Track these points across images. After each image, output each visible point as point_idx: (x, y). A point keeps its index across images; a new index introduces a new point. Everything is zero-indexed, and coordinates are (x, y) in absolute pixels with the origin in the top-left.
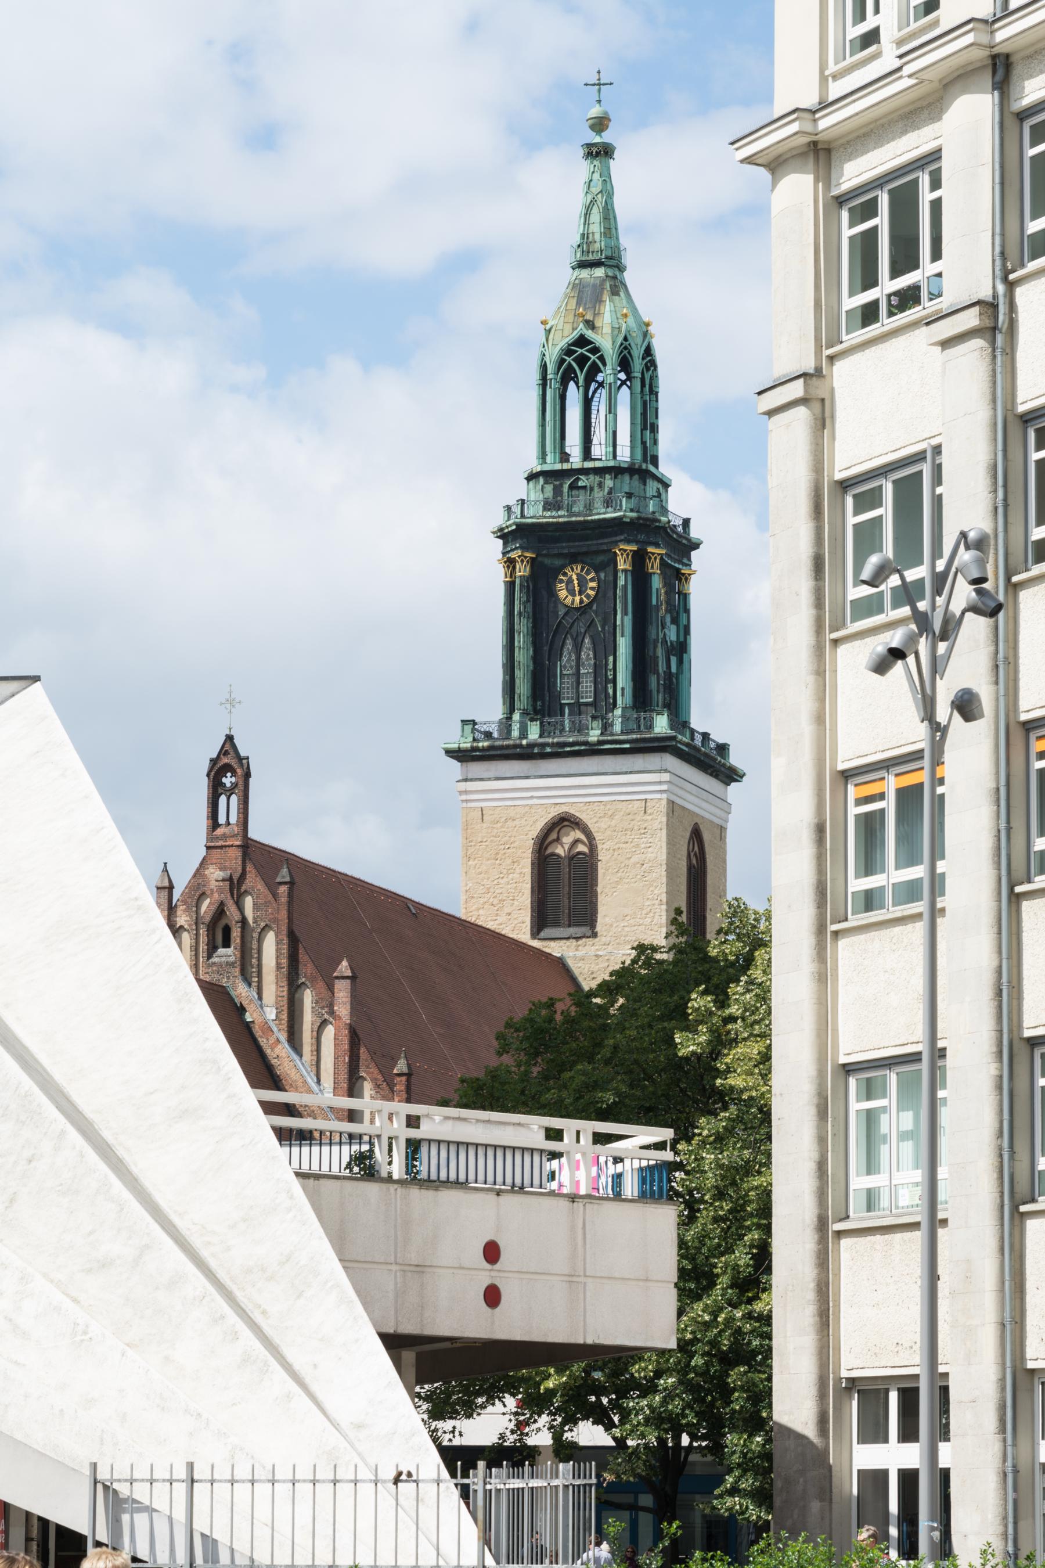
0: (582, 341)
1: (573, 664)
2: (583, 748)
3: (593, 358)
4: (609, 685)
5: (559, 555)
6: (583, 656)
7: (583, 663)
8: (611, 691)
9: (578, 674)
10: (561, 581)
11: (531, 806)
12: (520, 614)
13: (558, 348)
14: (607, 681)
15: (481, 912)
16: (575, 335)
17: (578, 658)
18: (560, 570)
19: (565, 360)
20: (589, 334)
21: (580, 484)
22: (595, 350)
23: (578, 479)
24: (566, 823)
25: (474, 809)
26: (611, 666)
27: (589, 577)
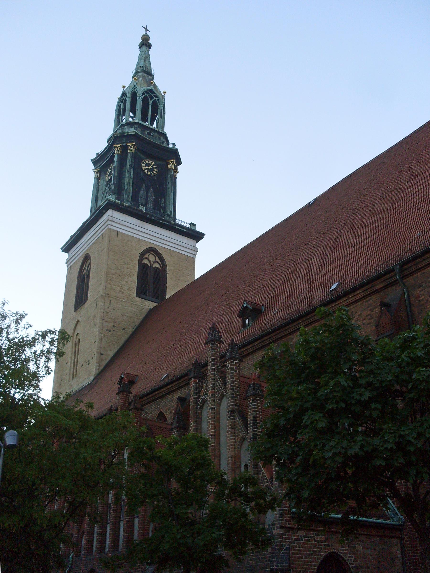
0: (151, 91)
1: (145, 195)
2: (167, 224)
3: (155, 98)
4: (162, 209)
5: (144, 153)
6: (149, 194)
7: (149, 197)
8: (162, 211)
9: (146, 200)
10: (144, 163)
11: (139, 240)
12: (131, 165)
13: (143, 89)
14: (162, 208)
15: (114, 276)
16: (150, 88)
17: (147, 193)
18: (142, 159)
19: (145, 94)
20: (154, 90)
21: (151, 134)
22: (156, 96)
23: (151, 132)
24: (152, 253)
25: (114, 231)
26: (163, 202)
27: (155, 167)
